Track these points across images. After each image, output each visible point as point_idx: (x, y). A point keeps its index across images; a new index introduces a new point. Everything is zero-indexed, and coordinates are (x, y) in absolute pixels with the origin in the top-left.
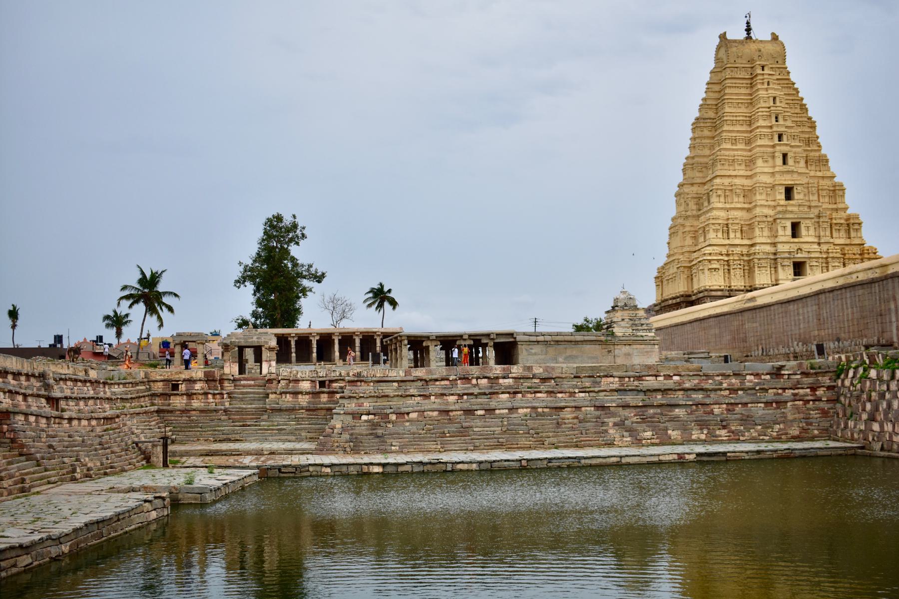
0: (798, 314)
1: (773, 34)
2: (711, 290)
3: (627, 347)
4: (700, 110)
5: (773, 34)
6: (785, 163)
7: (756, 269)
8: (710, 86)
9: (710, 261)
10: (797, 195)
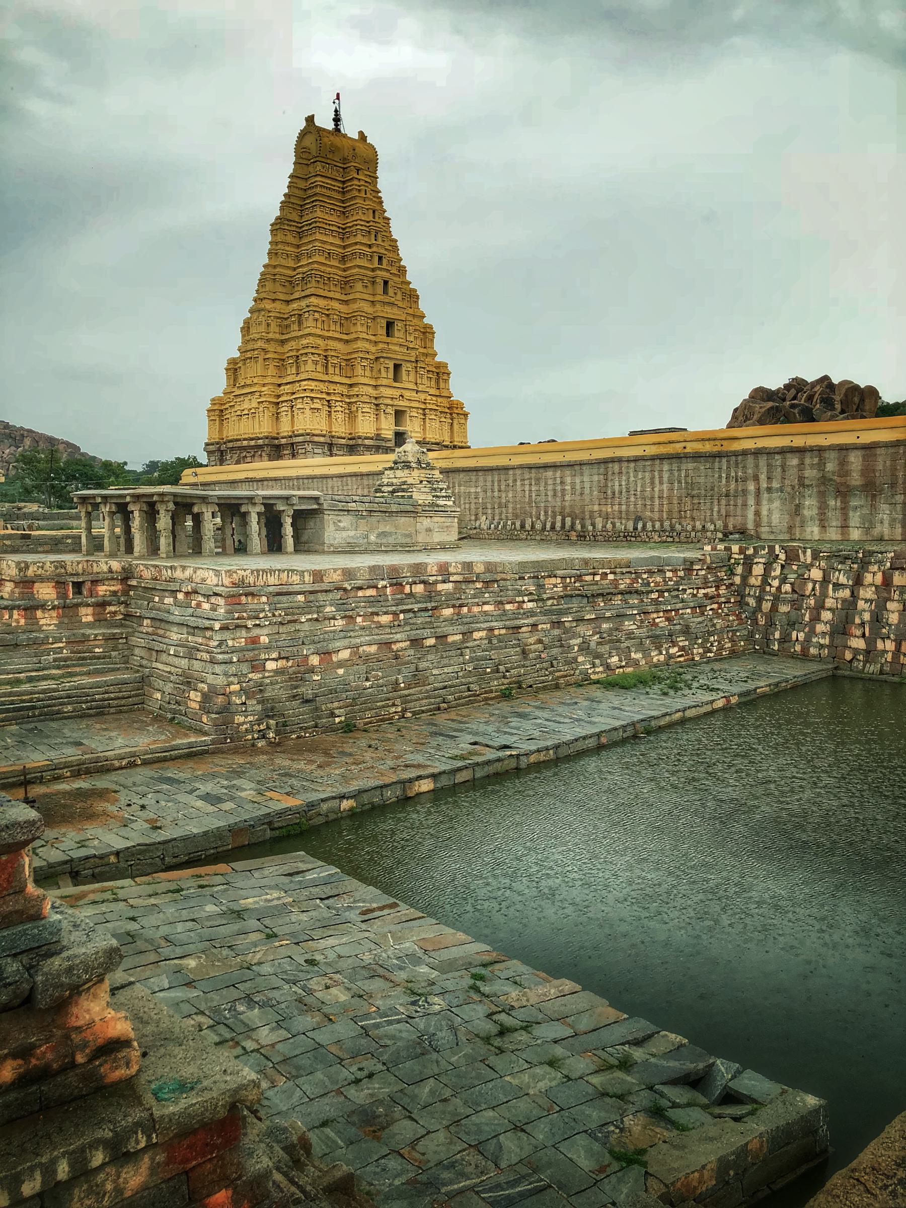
0: (562, 483)
1: (361, 133)
2: (314, 435)
3: (429, 520)
4: (282, 209)
5: (361, 133)
6: (385, 292)
7: (360, 414)
8: (294, 180)
9: (312, 398)
10: (398, 333)
